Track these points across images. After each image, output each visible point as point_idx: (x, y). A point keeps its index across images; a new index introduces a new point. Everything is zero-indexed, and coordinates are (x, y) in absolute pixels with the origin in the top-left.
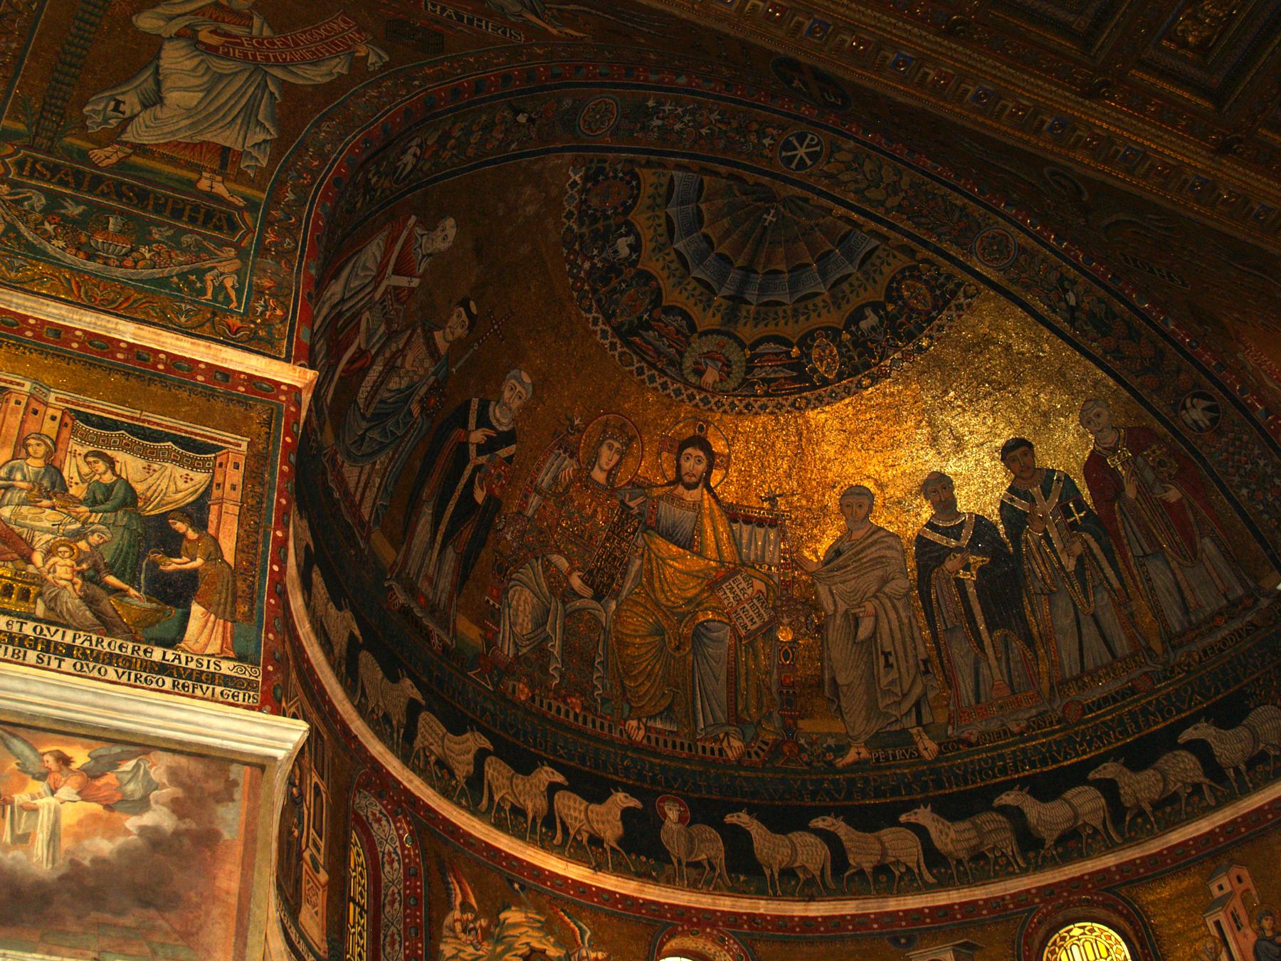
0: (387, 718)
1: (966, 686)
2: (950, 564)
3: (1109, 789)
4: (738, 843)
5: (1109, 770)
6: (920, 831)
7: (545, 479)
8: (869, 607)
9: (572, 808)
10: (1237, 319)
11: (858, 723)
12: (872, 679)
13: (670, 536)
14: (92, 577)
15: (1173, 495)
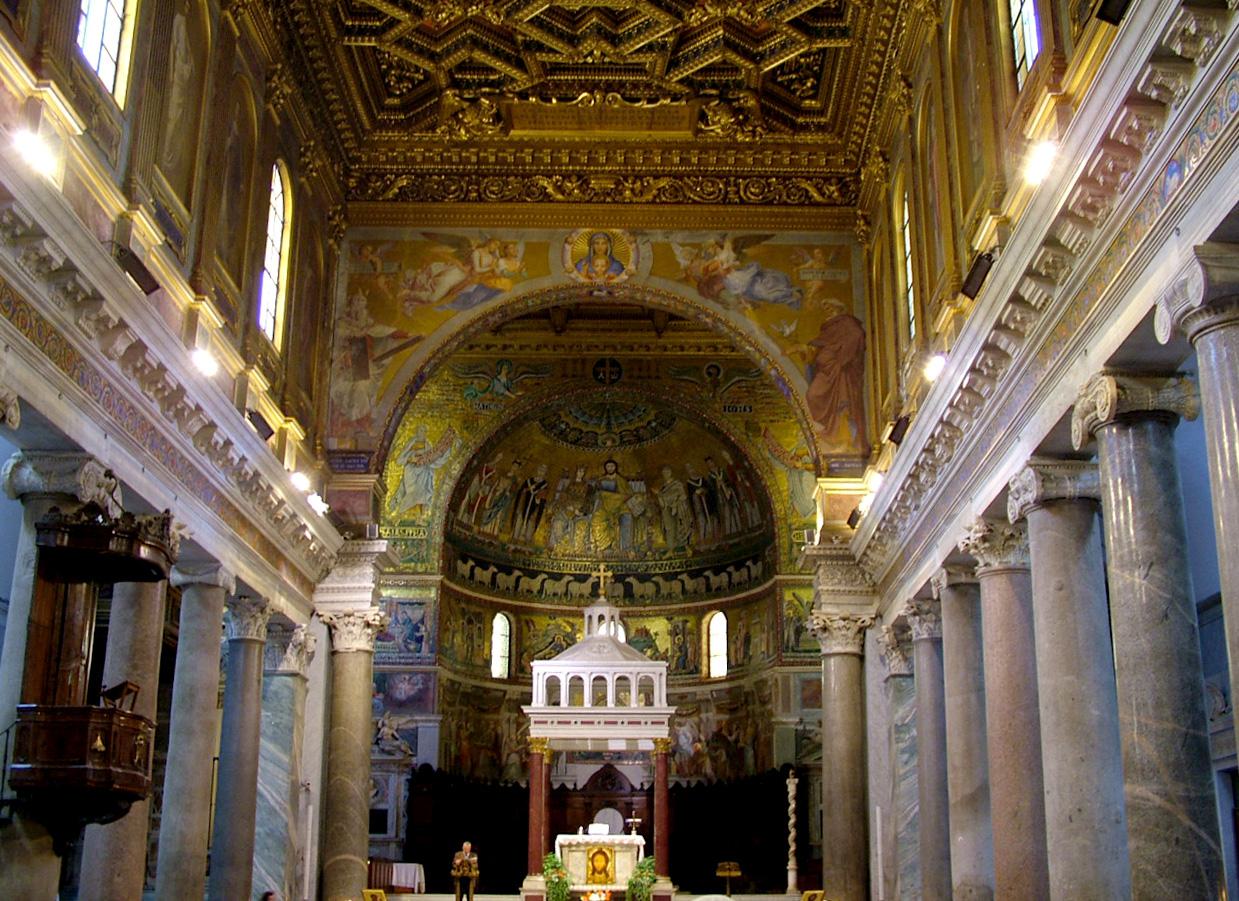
0: (508, 588)
1: (702, 532)
2: (698, 492)
3: (730, 574)
4: (628, 588)
5: (731, 569)
6: (682, 582)
7: (560, 488)
8: (674, 505)
9: (575, 587)
10: (772, 421)
11: (671, 544)
12: (676, 528)
13: (607, 490)
14: (405, 641)
15: (748, 484)
